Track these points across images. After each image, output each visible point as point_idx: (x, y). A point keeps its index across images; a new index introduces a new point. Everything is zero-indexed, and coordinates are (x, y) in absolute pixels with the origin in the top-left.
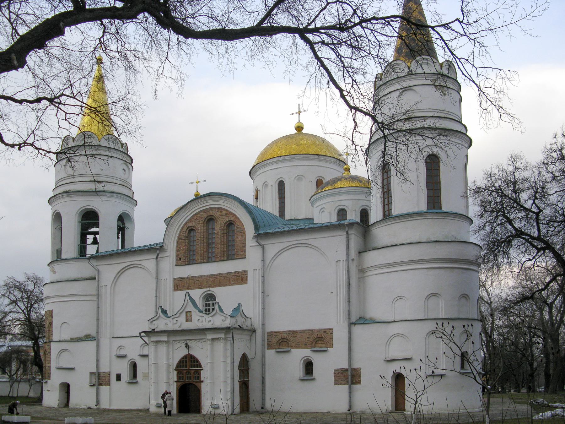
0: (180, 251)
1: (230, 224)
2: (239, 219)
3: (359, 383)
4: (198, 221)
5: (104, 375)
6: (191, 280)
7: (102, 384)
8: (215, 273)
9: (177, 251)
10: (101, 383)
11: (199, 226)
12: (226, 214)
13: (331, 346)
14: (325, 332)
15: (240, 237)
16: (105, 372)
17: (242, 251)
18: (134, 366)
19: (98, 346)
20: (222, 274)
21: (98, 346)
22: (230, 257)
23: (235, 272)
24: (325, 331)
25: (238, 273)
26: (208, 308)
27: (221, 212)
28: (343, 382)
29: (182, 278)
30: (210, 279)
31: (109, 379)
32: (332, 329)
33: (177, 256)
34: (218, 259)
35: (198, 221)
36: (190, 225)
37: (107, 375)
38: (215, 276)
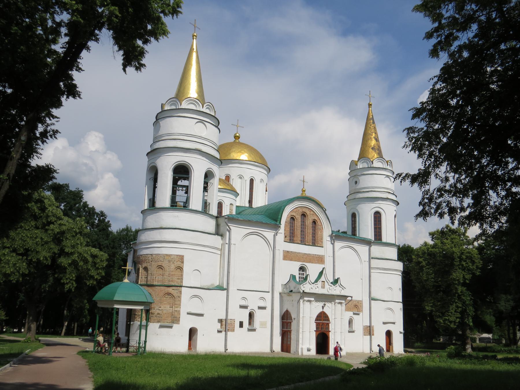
1: (314, 222)
2: (320, 219)
3: (373, 335)
4: (297, 213)
5: (231, 322)
7: (228, 330)
9: (285, 230)
10: (228, 329)
11: (298, 217)
12: (313, 214)
13: (362, 311)
14: (358, 302)
15: (319, 232)
16: (232, 319)
24: (358, 301)
26: (301, 276)
27: (310, 212)
28: (367, 334)
29: (288, 252)
32: (362, 301)
33: (284, 234)
34: (308, 244)
35: (297, 213)
36: (293, 214)
37: (233, 322)
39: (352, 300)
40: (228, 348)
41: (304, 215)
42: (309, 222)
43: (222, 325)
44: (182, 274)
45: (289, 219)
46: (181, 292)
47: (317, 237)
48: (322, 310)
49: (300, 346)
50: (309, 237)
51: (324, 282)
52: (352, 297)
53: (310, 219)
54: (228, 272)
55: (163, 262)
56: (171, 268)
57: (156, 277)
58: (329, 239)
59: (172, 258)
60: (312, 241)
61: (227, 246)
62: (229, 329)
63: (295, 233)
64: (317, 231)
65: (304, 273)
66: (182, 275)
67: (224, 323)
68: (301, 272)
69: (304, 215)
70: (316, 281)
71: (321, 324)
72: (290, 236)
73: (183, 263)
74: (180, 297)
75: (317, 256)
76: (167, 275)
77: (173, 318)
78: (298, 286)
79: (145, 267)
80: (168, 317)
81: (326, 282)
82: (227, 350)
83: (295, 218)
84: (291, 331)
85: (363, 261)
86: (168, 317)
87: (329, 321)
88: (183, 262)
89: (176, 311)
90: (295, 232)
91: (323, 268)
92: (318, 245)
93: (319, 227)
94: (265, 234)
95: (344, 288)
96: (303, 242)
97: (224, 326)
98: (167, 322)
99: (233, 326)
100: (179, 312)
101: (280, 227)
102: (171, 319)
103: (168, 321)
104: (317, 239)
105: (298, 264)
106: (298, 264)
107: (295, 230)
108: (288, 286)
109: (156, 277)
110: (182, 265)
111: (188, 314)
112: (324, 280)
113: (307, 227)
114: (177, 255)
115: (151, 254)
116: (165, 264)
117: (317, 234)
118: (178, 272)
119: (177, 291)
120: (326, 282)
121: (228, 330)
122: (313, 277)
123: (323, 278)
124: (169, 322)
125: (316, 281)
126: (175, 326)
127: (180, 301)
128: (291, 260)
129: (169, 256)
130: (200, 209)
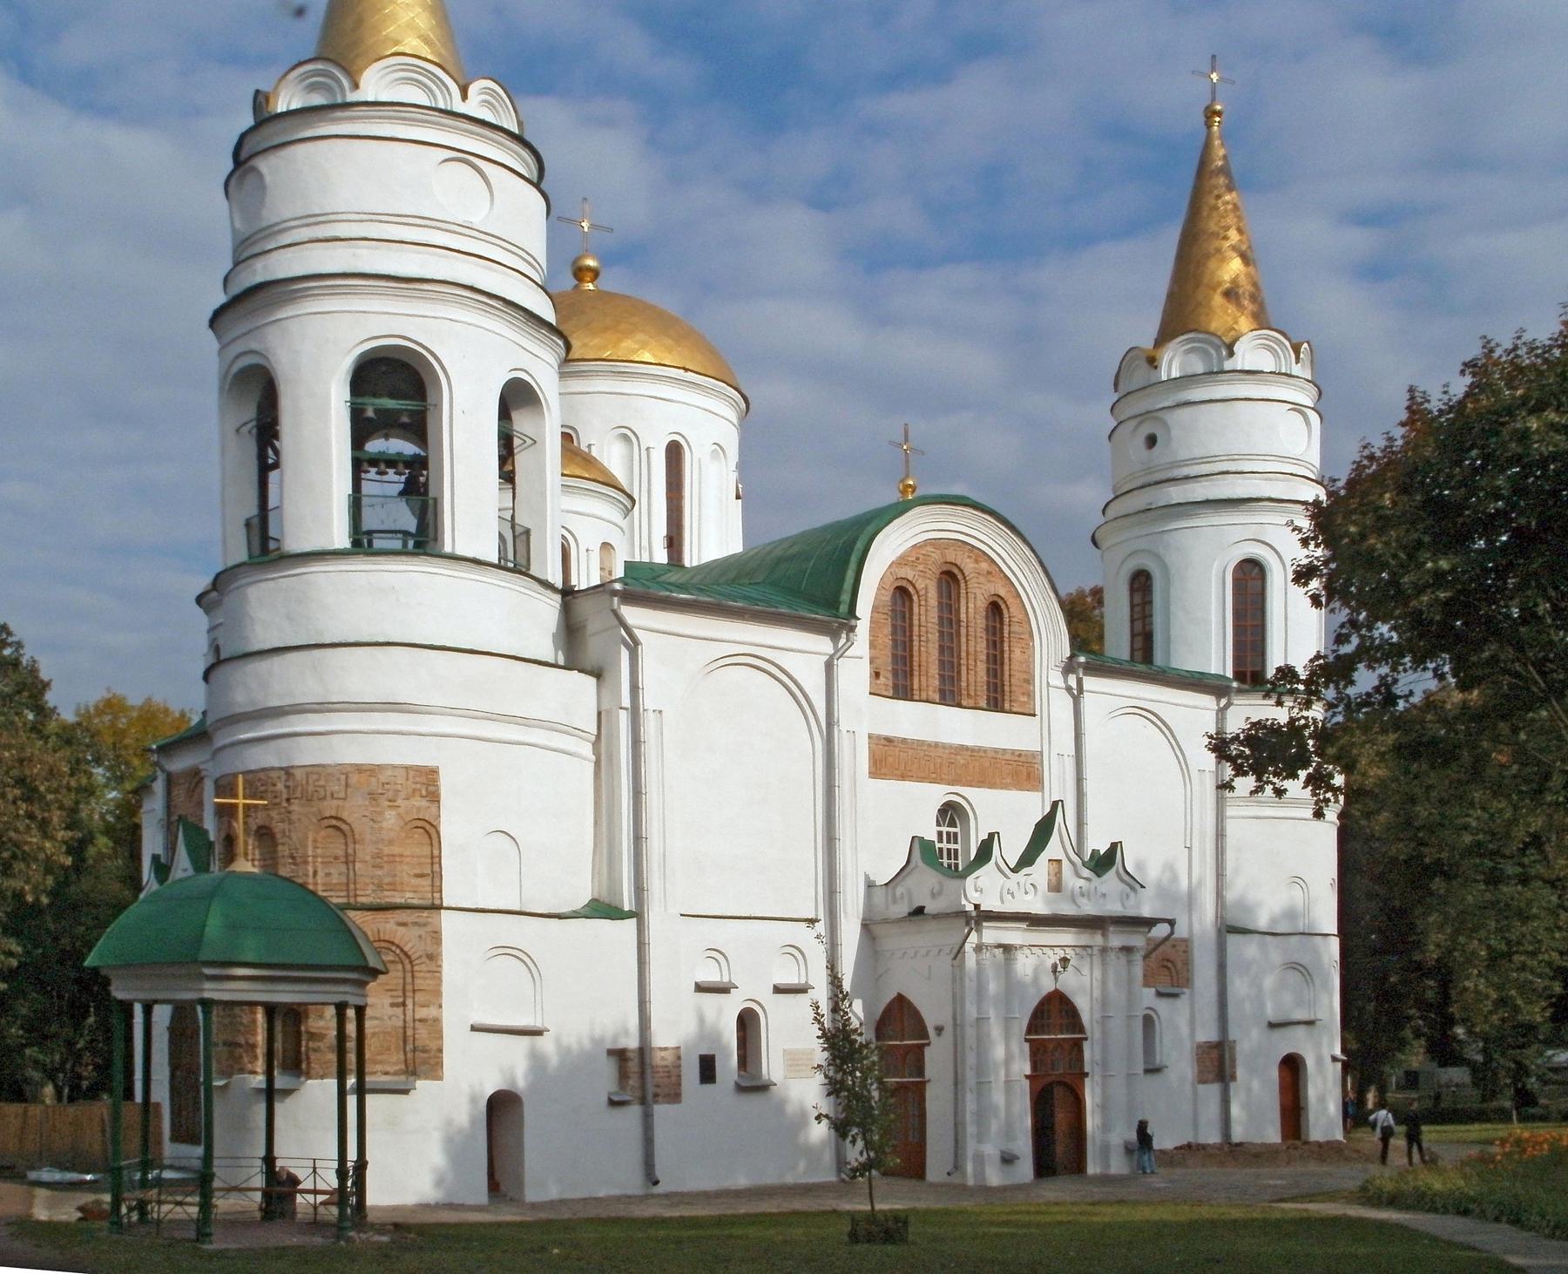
0: (875, 649)
6: (911, 752)
8: (969, 743)
9: (872, 645)
15: (1017, 654)
17: (1023, 694)
18: (747, 1022)
19: (642, 946)
20: (985, 751)
21: (642, 946)
22: (997, 701)
23: (1013, 752)
25: (1020, 755)
29: (889, 740)
30: (959, 757)
31: (679, 1076)
34: (971, 703)
35: (921, 567)
38: (969, 753)
39: (1172, 933)
40: (659, 1173)
41: (950, 579)
42: (971, 605)
43: (623, 1075)
44: (436, 852)
45: (887, 597)
46: (436, 936)
47: (1007, 673)
48: (1053, 989)
49: (971, 1147)
50: (976, 674)
51: (1059, 861)
52: (1172, 923)
53: (980, 597)
54: (638, 839)
55: (345, 799)
56: (385, 824)
57: (315, 873)
58: (1056, 678)
59: (383, 779)
60: (988, 690)
61: (624, 719)
62: (659, 1091)
63: (916, 659)
64: (1006, 648)
65: (955, 834)
66: (435, 860)
67: (633, 1066)
68: (945, 829)
69: (950, 579)
70: (1027, 859)
71: (1051, 1046)
72: (895, 673)
73: (439, 801)
74: (434, 957)
75: (1008, 757)
76: (368, 858)
77: (410, 1055)
78: (952, 884)
79: (260, 828)
80: (388, 1049)
81: (1065, 863)
82: (656, 1183)
83: (911, 589)
84: (923, 1084)
85: (1195, 774)
86: (388, 1049)
87: (1081, 1029)
88: (434, 798)
89: (420, 1020)
90: (915, 653)
91: (1055, 805)
92: (1014, 710)
93: (1015, 628)
94: (786, 660)
95: (1138, 887)
96: (950, 695)
97: (633, 1082)
98: (386, 1073)
99: (674, 1079)
100: (435, 1025)
101: (852, 629)
102: (402, 1057)
103: (388, 1069)
104: (1007, 683)
105: (937, 794)
106: (937, 794)
107: (916, 643)
108: (899, 890)
109: (315, 873)
110: (434, 809)
111: (474, 1028)
112: (1060, 855)
113: (963, 631)
114: (407, 768)
115: (282, 769)
116: (354, 811)
117: (1006, 661)
118: (415, 848)
119: (422, 931)
120: (1065, 863)
121: (656, 1095)
122: (1013, 846)
123: (1053, 849)
124: (396, 1073)
125: (1027, 859)
126: (419, 1083)
127: (436, 974)
128: (903, 777)
129: (372, 770)
130: (494, 558)
